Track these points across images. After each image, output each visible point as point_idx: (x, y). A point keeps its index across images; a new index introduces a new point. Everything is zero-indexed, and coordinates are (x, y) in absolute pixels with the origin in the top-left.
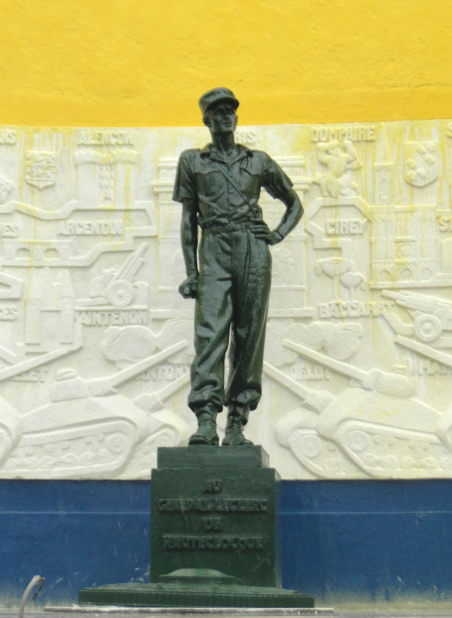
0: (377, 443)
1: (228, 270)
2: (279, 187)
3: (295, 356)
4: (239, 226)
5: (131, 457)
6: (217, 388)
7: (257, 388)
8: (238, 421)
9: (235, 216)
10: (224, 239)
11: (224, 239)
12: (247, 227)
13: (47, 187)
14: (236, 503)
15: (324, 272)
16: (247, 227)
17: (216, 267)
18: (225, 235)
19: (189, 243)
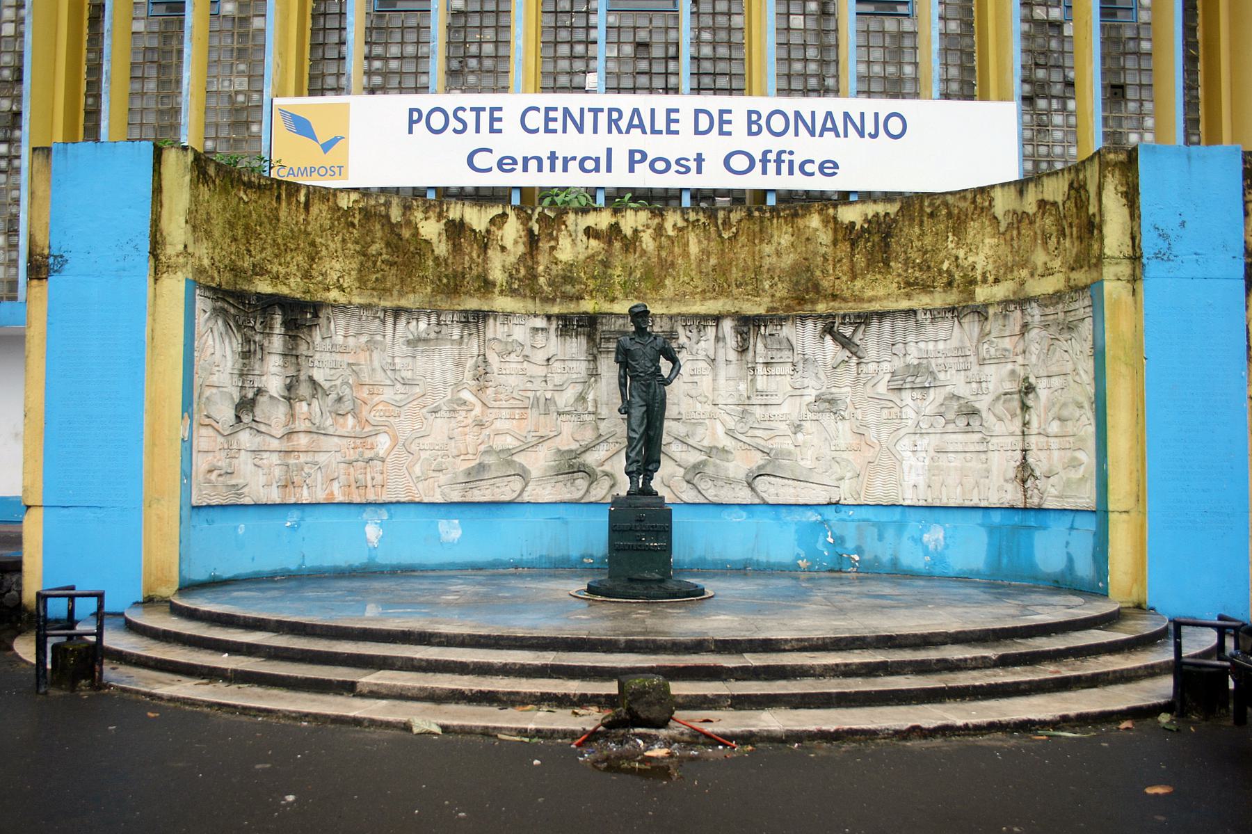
5: (587, 491)
7: (659, 462)
8: (649, 477)
17: (638, 399)
19: (622, 385)
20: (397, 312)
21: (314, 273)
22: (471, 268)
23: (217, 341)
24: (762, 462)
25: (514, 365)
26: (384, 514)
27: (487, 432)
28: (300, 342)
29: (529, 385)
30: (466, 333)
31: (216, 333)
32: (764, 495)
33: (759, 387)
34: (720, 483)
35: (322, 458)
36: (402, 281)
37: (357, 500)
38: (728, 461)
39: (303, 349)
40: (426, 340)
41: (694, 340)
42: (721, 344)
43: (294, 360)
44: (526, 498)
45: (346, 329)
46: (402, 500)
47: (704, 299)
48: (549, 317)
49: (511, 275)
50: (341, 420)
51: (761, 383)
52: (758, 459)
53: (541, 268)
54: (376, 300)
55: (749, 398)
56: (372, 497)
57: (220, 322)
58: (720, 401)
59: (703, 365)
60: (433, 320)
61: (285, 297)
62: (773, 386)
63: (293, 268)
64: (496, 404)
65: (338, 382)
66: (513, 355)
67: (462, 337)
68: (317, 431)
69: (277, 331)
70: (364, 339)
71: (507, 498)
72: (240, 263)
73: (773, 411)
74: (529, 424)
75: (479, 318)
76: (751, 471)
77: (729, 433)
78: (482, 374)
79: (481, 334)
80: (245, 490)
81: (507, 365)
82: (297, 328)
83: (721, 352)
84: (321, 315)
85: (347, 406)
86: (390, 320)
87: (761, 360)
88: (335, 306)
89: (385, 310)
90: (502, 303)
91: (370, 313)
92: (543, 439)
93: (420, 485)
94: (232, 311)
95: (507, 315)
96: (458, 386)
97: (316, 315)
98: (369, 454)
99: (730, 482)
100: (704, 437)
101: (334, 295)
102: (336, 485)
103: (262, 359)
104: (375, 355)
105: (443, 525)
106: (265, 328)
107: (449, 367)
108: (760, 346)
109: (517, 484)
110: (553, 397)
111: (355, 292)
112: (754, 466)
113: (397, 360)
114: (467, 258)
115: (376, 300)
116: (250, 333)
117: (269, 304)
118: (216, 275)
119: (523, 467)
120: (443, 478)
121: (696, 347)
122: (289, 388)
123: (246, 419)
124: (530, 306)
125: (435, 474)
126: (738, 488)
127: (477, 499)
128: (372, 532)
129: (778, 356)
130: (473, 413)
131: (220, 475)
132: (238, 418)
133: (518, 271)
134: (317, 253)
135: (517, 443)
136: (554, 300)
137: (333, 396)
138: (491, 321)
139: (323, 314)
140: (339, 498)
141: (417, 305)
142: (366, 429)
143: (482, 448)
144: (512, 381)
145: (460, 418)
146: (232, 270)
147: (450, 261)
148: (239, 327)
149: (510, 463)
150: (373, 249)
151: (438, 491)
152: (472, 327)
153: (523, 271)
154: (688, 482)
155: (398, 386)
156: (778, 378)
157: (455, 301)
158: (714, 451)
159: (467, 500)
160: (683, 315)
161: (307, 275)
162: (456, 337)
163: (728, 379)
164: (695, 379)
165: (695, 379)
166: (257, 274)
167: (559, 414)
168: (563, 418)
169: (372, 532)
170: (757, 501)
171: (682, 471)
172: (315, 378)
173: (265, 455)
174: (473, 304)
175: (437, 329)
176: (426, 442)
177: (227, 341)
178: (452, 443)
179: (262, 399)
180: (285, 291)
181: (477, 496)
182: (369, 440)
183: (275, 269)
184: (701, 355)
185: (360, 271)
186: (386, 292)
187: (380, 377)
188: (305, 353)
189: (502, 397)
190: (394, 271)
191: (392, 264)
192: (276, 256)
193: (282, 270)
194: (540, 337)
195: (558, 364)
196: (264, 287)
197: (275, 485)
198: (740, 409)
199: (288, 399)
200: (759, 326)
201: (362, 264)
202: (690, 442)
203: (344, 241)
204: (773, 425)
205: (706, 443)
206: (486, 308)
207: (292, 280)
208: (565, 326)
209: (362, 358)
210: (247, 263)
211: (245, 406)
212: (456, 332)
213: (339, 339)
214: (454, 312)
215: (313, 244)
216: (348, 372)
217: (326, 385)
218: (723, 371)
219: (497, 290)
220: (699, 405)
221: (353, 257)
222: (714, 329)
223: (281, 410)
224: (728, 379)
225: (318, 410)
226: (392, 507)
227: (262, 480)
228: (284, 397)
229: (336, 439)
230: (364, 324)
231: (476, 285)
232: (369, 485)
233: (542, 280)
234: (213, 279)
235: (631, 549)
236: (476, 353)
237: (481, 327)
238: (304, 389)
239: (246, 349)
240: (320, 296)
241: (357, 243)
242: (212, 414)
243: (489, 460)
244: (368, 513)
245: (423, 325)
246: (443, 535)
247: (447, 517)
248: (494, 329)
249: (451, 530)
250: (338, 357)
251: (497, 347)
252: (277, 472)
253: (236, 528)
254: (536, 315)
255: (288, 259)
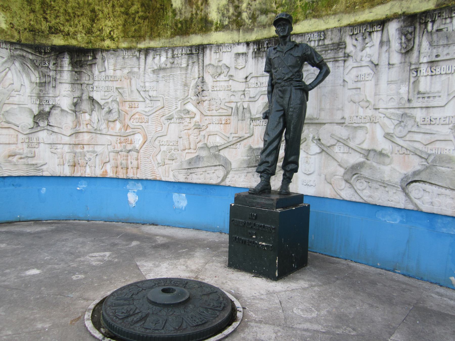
0: (370, 187)
1: (282, 106)
2: (312, 61)
3: (336, 141)
4: (286, 84)
6: (269, 165)
9: (285, 79)
10: (280, 90)
11: (280, 90)
12: (291, 84)
13: (242, 68)
14: (261, 226)
15: (351, 100)
16: (291, 84)
18: (280, 88)
20: (147, 51)
21: (94, 30)
22: (197, 14)
23: (15, 75)
24: (418, 168)
25: (223, 84)
26: (140, 187)
27: (202, 133)
28: (83, 75)
29: (232, 98)
30: (190, 62)
31: (13, 71)
32: (418, 202)
33: (422, 88)
34: (375, 185)
35: (98, 149)
36: (152, 29)
37: (121, 176)
38: (384, 164)
39: (85, 79)
40: (164, 69)
41: (359, 48)
42: (385, 48)
43: (79, 86)
44: (227, 182)
45: (115, 65)
46: (149, 178)
47: (373, 6)
48: (248, 44)
49: (223, 15)
50: (111, 124)
51: (424, 84)
52: (415, 164)
53: (244, 5)
54: (134, 44)
55: (409, 101)
56: (131, 175)
57: (17, 64)
58: (381, 105)
59: (367, 71)
60: (170, 55)
61: (74, 47)
62: (437, 87)
63: (80, 28)
64: (209, 113)
65: (109, 101)
66: (222, 76)
67: (188, 65)
68: (96, 132)
69: (66, 69)
70: (126, 71)
71: (214, 182)
72: (37, 27)
73: (435, 114)
74: (231, 128)
75: (201, 48)
76: (406, 176)
77: (388, 136)
78: (200, 92)
79: (201, 61)
80: (44, 167)
81: (218, 84)
82: (81, 67)
83: (384, 57)
84: (97, 57)
85: (114, 116)
86: (142, 57)
87: (425, 60)
88: (107, 50)
89: (140, 50)
90: (216, 37)
91: (129, 53)
92: (241, 139)
93: (160, 169)
94: (31, 57)
95: (219, 46)
96: (185, 101)
97: (94, 58)
98: (129, 147)
99: (384, 184)
100: (363, 140)
101: (107, 43)
102: (108, 167)
103: (55, 87)
104: (133, 82)
105: (175, 196)
106: (57, 67)
107: (180, 87)
108: (425, 44)
109: (221, 172)
110: (249, 107)
111: (121, 40)
112: (410, 171)
113: (147, 84)
114: (194, 7)
115: (134, 44)
116: (45, 70)
117: (59, 51)
118: (16, 34)
119: (226, 160)
120: (174, 165)
121: (360, 54)
122: (75, 105)
123: (42, 124)
124: (235, 36)
125: (170, 162)
126: (392, 191)
127: (194, 181)
128: (132, 198)
129: (443, 53)
130: (194, 119)
131: (21, 158)
132: (36, 123)
133: (228, 10)
134: (96, 16)
135: (222, 142)
136: (252, 30)
137: (106, 109)
138: (208, 52)
139: (99, 56)
140: (110, 174)
141: (161, 45)
142: (128, 131)
143: (200, 145)
144: (222, 95)
145: (186, 124)
146: (32, 31)
147: (183, 11)
148: (36, 67)
149: (216, 156)
150: (133, 10)
151: (171, 173)
152: (195, 57)
153: (231, 10)
154: (347, 181)
155: (148, 101)
156: (444, 77)
157: (186, 39)
158: (372, 154)
159: (189, 181)
160: (349, 25)
161: (89, 32)
162: (184, 65)
163: (390, 83)
164: (359, 85)
165: (359, 85)
166: (52, 33)
167: (252, 120)
168: (254, 123)
169: (132, 198)
170: (410, 207)
171: (341, 171)
172: (95, 98)
173: (59, 146)
174: (196, 40)
175: (171, 60)
176: (165, 139)
177: (24, 76)
178: (181, 141)
179: (56, 112)
180: (74, 43)
181: (195, 179)
182: (130, 138)
183: (66, 29)
184: (366, 60)
185: (124, 25)
186: (140, 37)
187: (136, 96)
188: (87, 82)
189: (214, 107)
190: (146, 23)
191: (144, 18)
192: (67, 21)
193: (72, 30)
194: (241, 60)
195: (253, 81)
196: (58, 41)
197: (66, 165)
198: (400, 112)
199: (75, 112)
200: (426, 24)
201: (125, 21)
202: (352, 144)
203: (113, 6)
204: (434, 128)
205: (365, 146)
206: (205, 42)
207: (79, 35)
208: (259, 49)
209: (125, 83)
210: (44, 26)
211: (42, 116)
212: (183, 61)
213: (110, 72)
214: (182, 47)
215: (93, 11)
216: (116, 93)
217: (102, 102)
218: (385, 75)
219: (213, 28)
220: (361, 110)
221: (119, 16)
222: (379, 34)
223: (69, 120)
224: (390, 83)
225: (96, 118)
226: (145, 182)
227: (57, 161)
228: (71, 110)
229: (109, 137)
230: (126, 61)
231: (200, 26)
232: (130, 167)
233: (245, 15)
234: (13, 37)
235: (244, 242)
236: (197, 76)
237: (201, 57)
238: (85, 106)
239: (43, 80)
240: (98, 45)
241: (122, 6)
242: (11, 121)
243: (204, 153)
244: (129, 186)
245: (163, 59)
246: (176, 204)
247: (179, 193)
248: (210, 57)
249: (181, 200)
250: (109, 84)
251: (211, 70)
252: (68, 157)
253: (39, 190)
254: (239, 43)
255: (76, 22)
